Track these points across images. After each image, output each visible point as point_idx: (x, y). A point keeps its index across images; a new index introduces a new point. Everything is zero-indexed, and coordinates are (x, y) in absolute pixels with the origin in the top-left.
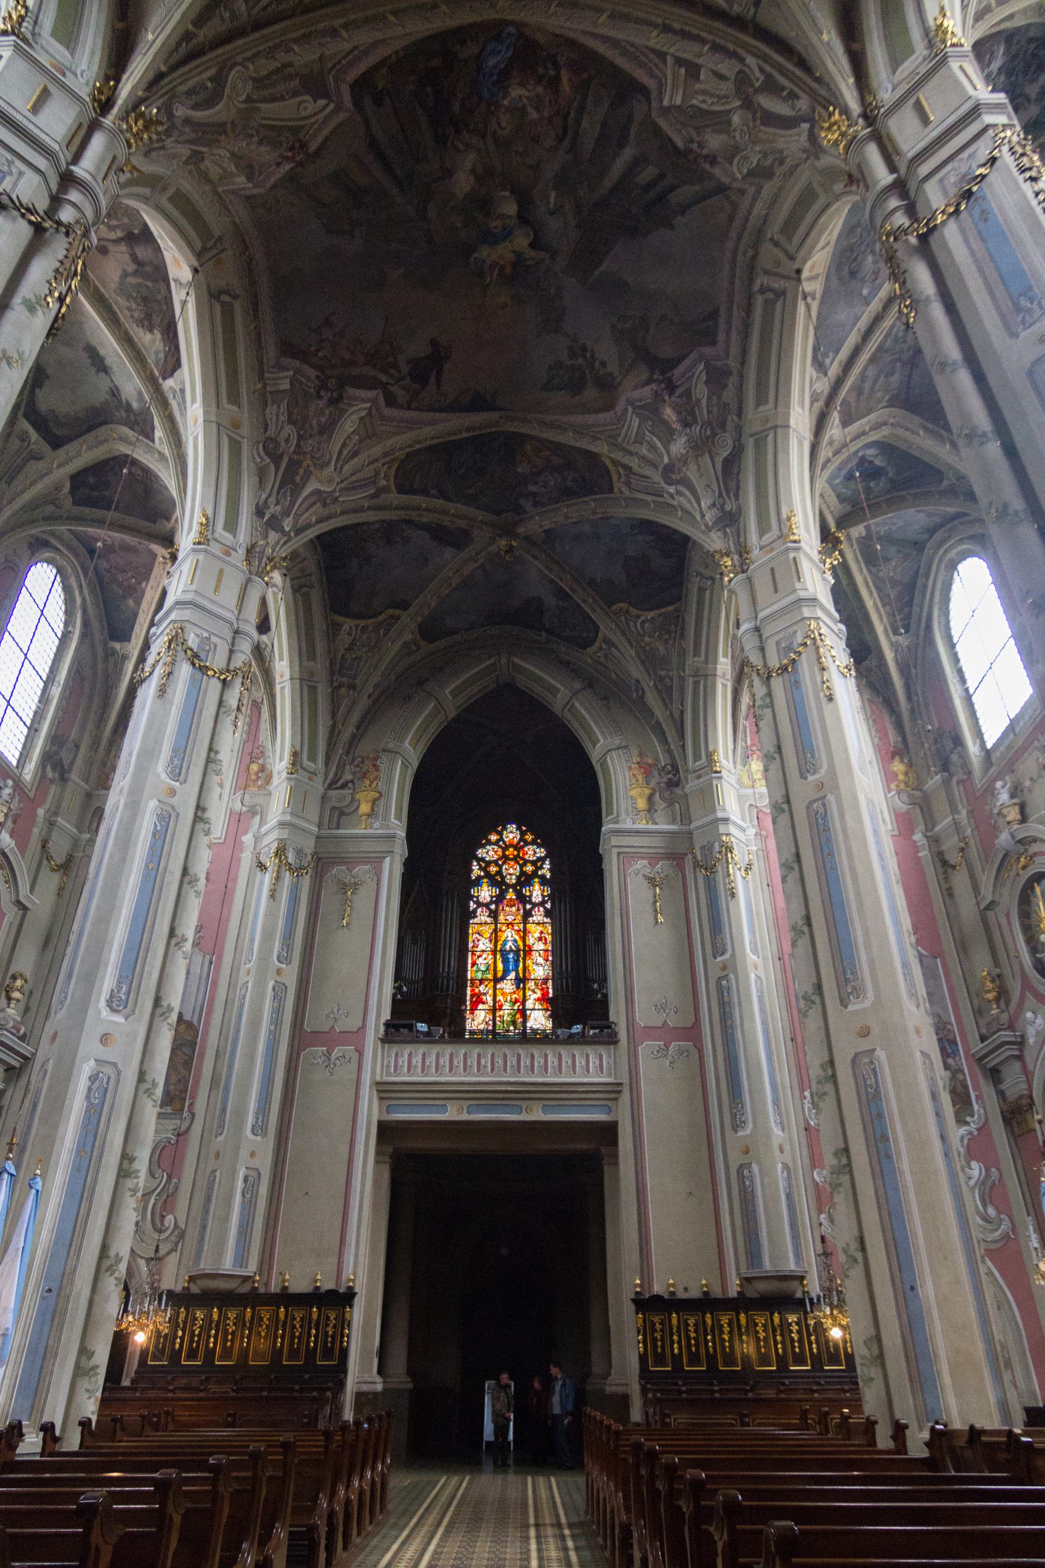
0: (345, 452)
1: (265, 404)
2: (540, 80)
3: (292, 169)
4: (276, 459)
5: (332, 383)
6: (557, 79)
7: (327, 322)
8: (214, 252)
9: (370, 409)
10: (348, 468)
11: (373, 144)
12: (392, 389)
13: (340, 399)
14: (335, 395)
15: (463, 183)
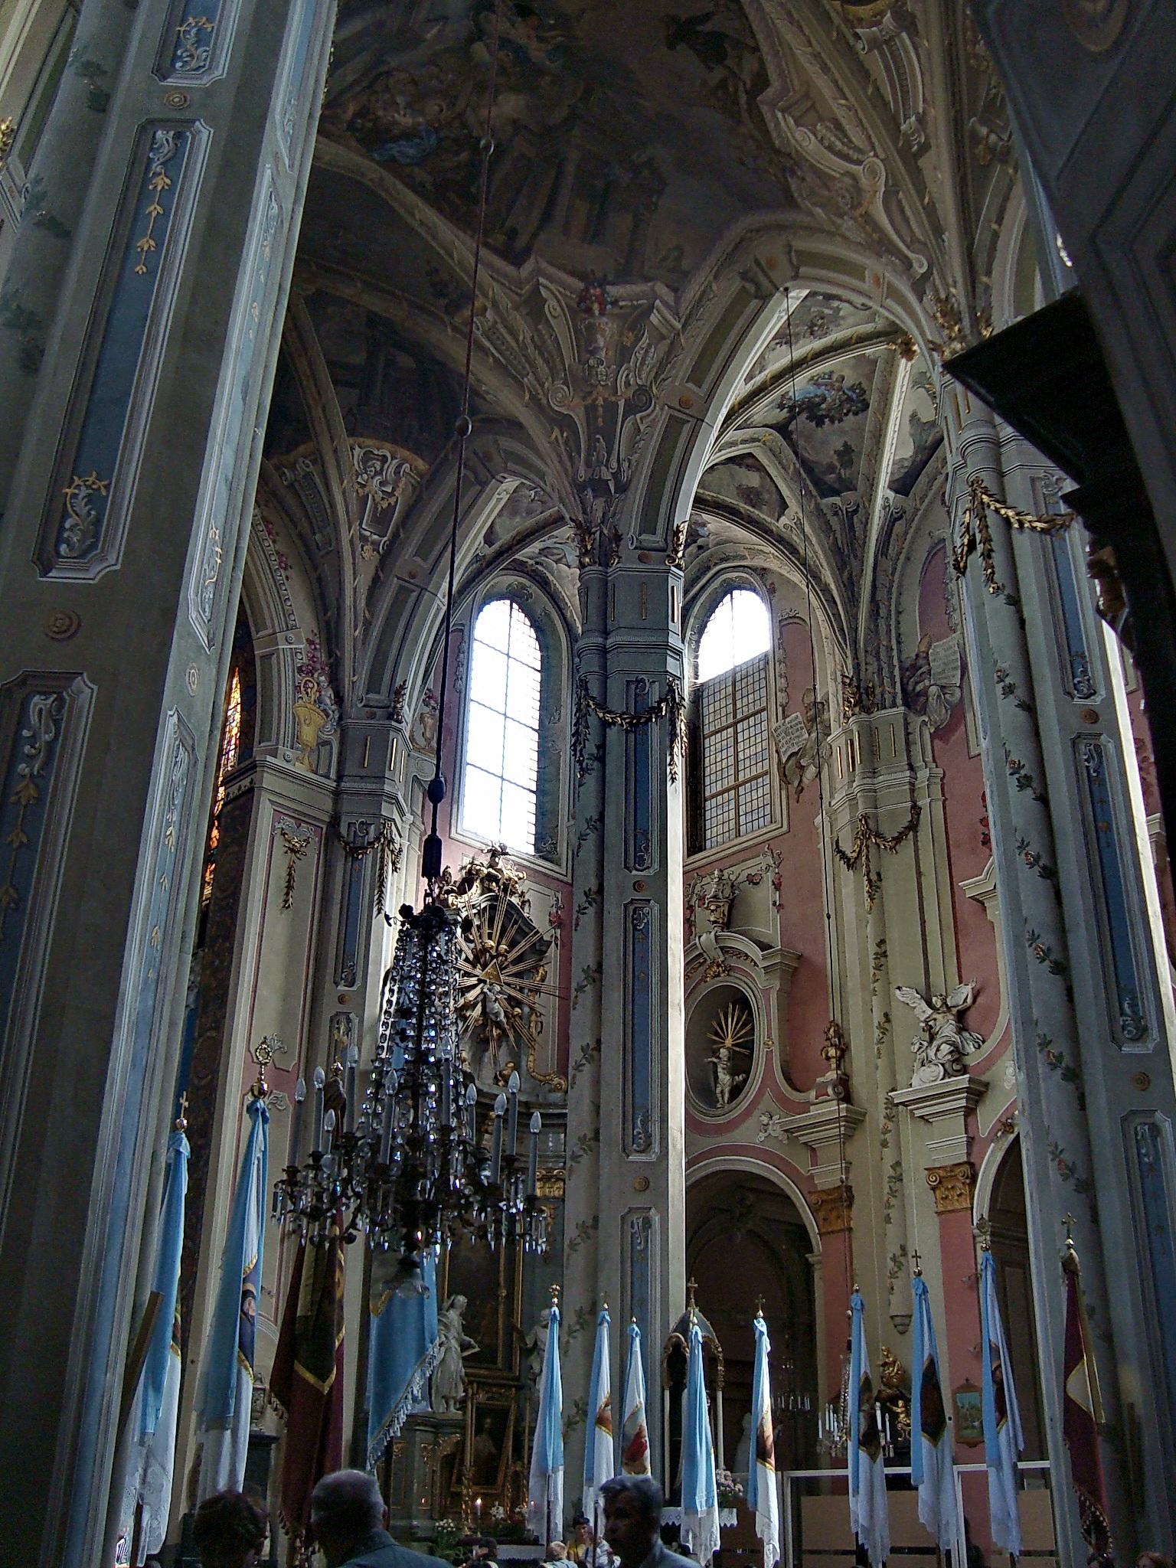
0: (839, 145)
2: (378, 118)
3: (613, 284)
6: (356, 115)
7: (743, 163)
8: (762, 278)
9: (783, 111)
10: (858, 140)
11: (547, 217)
12: (748, 86)
15: (510, 105)
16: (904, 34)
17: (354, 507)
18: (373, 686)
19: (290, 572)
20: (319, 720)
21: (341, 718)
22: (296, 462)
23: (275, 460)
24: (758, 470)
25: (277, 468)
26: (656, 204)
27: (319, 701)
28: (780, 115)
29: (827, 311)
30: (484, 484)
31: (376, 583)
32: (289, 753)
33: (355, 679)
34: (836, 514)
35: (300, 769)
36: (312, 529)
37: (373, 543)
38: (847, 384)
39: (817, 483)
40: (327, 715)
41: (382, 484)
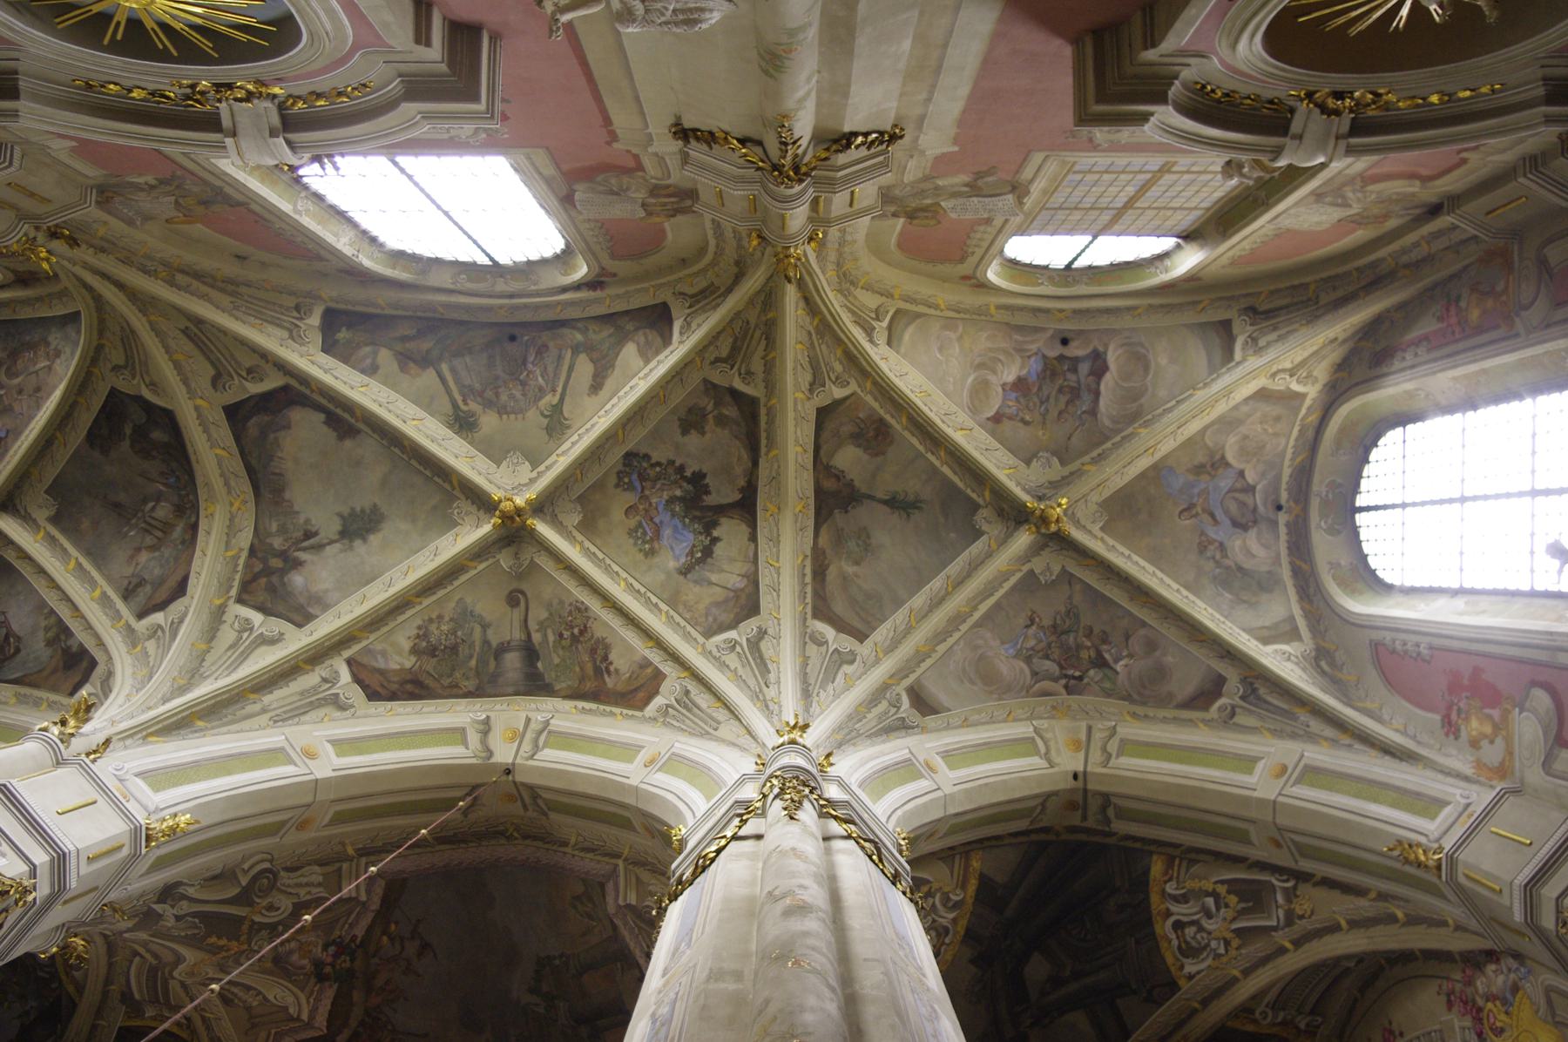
1: (322, 863)
4: (244, 898)
5: (345, 962)
7: (425, 947)
9: (298, 1019)
13: (321, 978)
14: (328, 969)
16: (137, 996)
17: (1258, 948)
24: (828, 468)
26: (561, 956)
28: (305, 1017)
29: (551, 638)
30: (1106, 798)
34: (749, 373)
37: (1289, 900)
38: (630, 498)
39: (753, 417)
41: (1209, 916)
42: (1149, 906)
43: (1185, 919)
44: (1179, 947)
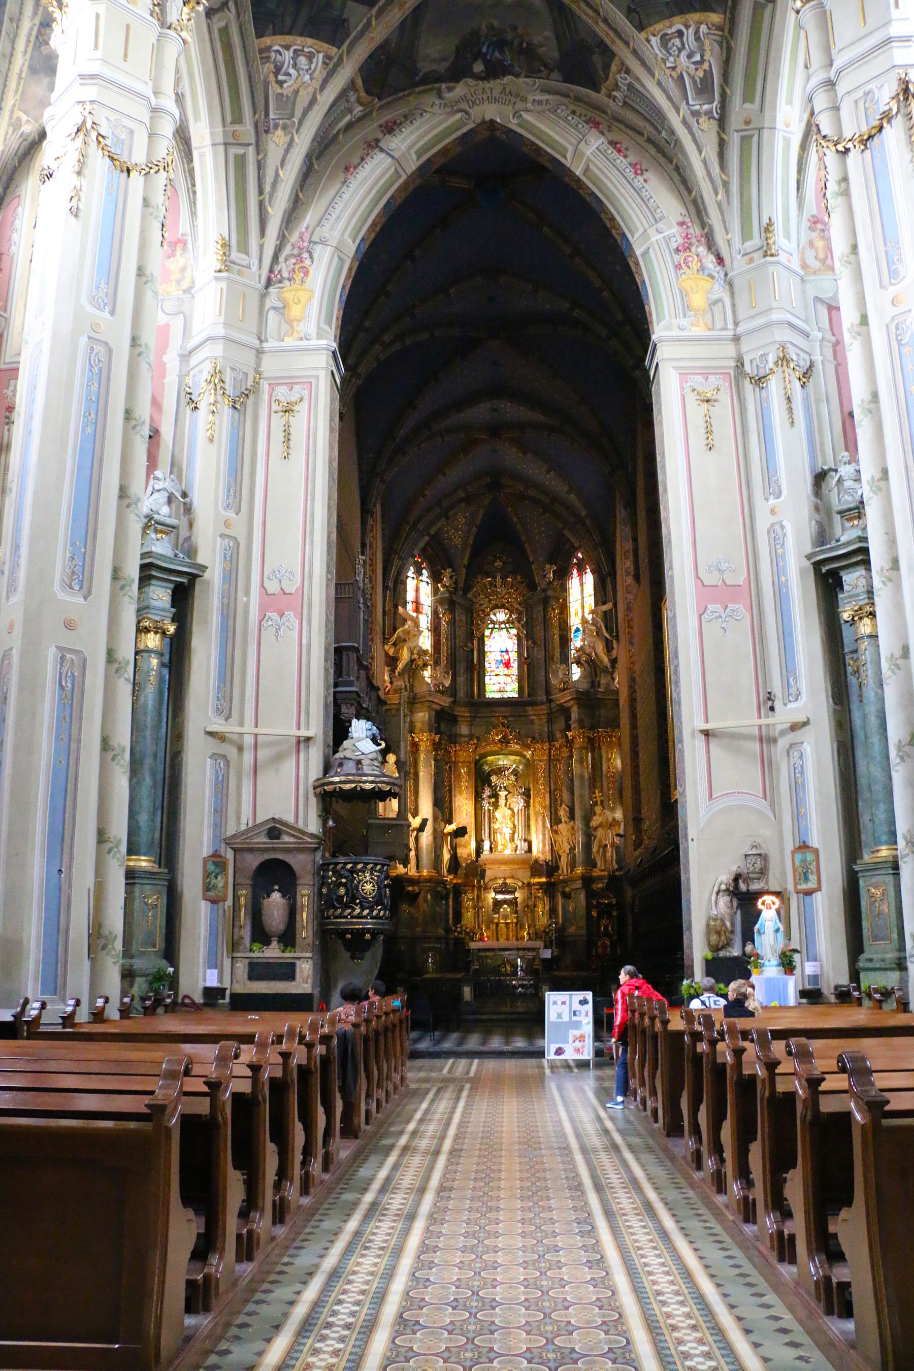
18: (746, 235)
19: (647, 175)
20: (705, 284)
21: (726, 275)
22: (616, 80)
23: (604, 90)
25: (609, 96)
27: (702, 269)
31: (722, 145)
32: (683, 322)
33: (729, 237)
35: (698, 331)
36: (656, 128)
40: (712, 277)
41: (689, 56)
42: (689, 12)
43: (685, 39)
44: (666, 34)
